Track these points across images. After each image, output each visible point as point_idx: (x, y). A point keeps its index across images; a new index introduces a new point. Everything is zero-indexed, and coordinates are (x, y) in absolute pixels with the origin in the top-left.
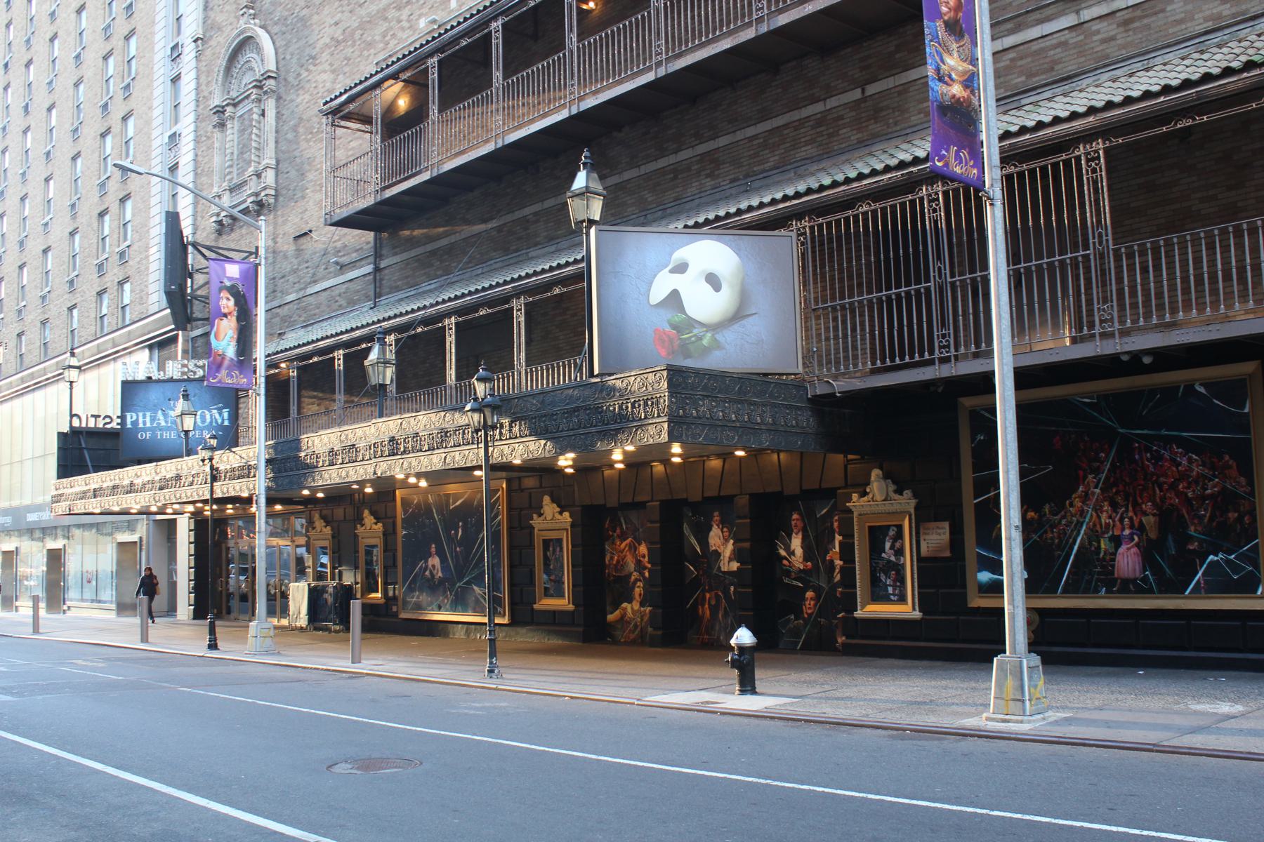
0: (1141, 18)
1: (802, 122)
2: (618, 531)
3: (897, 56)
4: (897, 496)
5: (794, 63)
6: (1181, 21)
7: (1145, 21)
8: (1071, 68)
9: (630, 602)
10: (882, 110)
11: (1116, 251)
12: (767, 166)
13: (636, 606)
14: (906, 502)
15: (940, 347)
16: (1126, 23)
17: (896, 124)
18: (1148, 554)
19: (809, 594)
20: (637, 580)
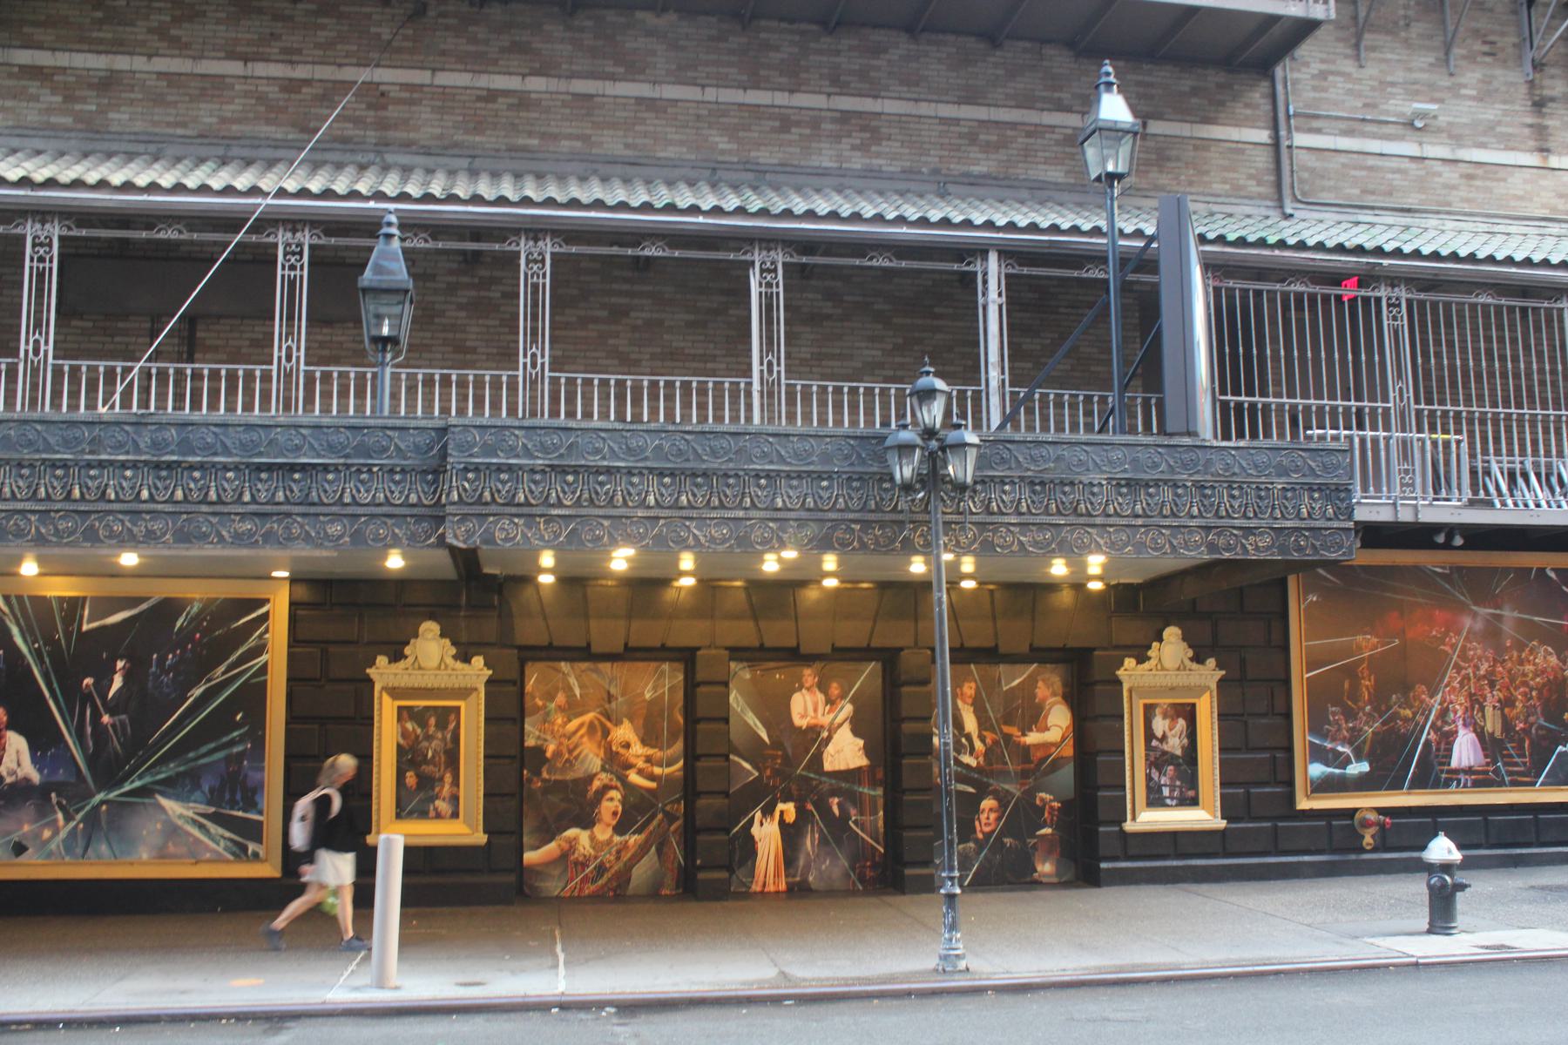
0: (1484, 178)
1: (1036, 131)
2: (561, 698)
3: (1194, 100)
4: (1195, 666)
5: (1028, 45)
6: (1521, 198)
7: (1488, 183)
8: (1412, 201)
9: (587, 822)
10: (1169, 159)
11: (58, 372)
12: (976, 169)
13: (603, 833)
14: (1209, 674)
15: (1402, 485)
16: (1470, 177)
17: (1191, 184)
18: (1488, 744)
19: (988, 803)
20: (606, 788)
